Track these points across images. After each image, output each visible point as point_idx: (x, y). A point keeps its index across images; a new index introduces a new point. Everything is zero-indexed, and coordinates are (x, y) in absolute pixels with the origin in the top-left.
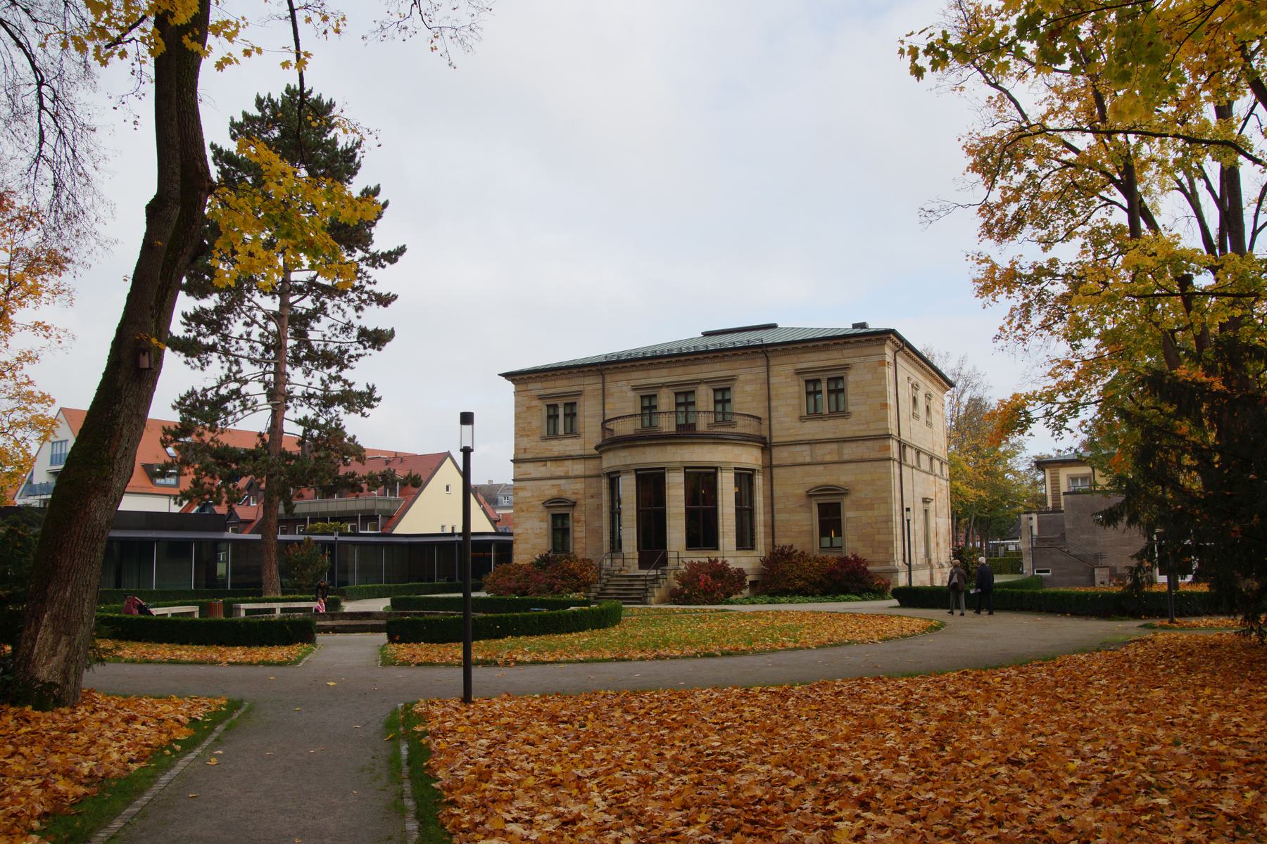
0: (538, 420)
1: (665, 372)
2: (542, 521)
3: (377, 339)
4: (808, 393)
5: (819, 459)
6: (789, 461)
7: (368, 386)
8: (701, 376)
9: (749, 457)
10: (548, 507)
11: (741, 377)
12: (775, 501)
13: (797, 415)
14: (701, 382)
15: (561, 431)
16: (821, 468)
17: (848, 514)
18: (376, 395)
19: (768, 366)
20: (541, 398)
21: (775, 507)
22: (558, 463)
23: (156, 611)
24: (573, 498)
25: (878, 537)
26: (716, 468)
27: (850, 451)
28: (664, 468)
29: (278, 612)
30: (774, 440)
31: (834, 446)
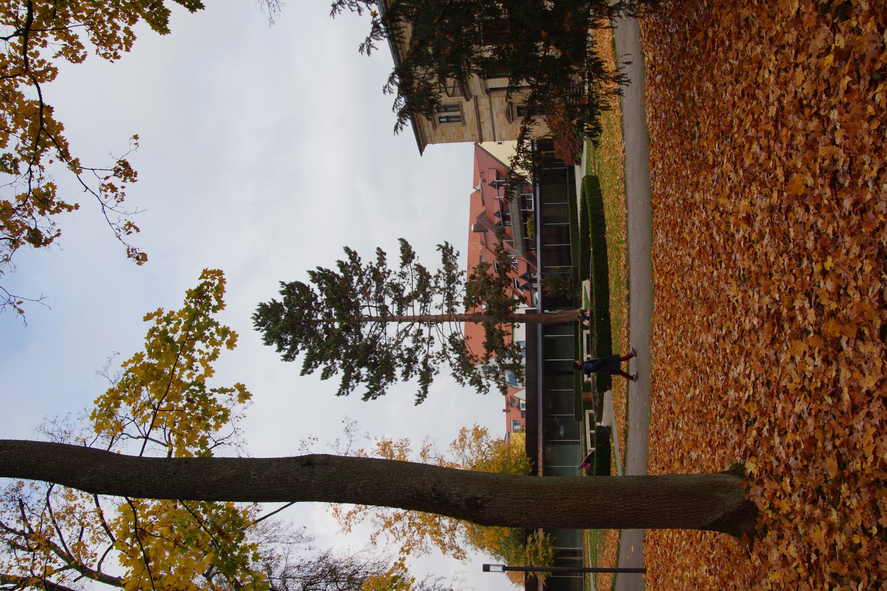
0: (452, 128)
3: (407, 254)
7: (438, 250)
10: (513, 119)
15: (458, 114)
18: (444, 244)
23: (586, 284)
29: (589, 356)
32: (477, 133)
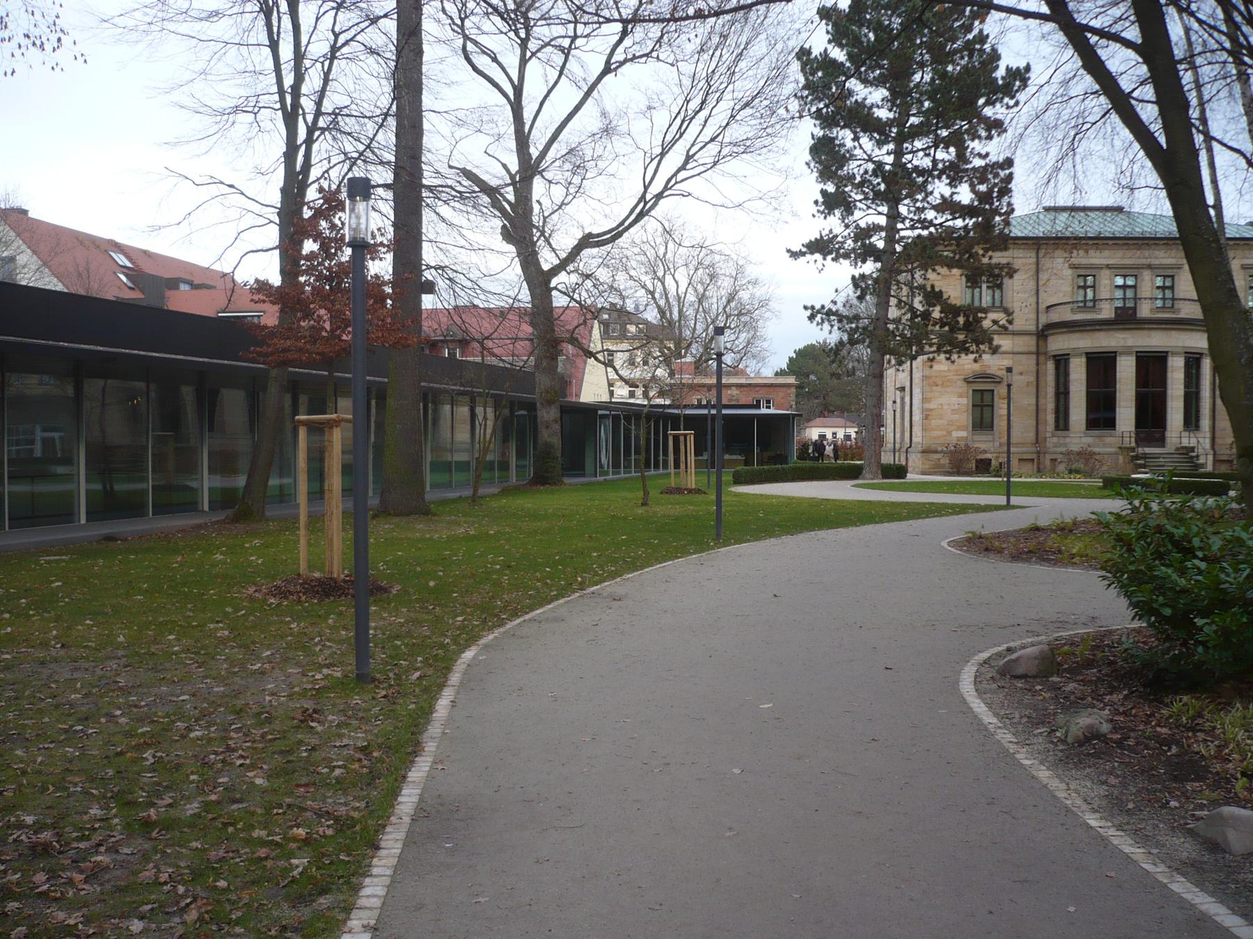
2: (961, 396)
28: (1167, 352)
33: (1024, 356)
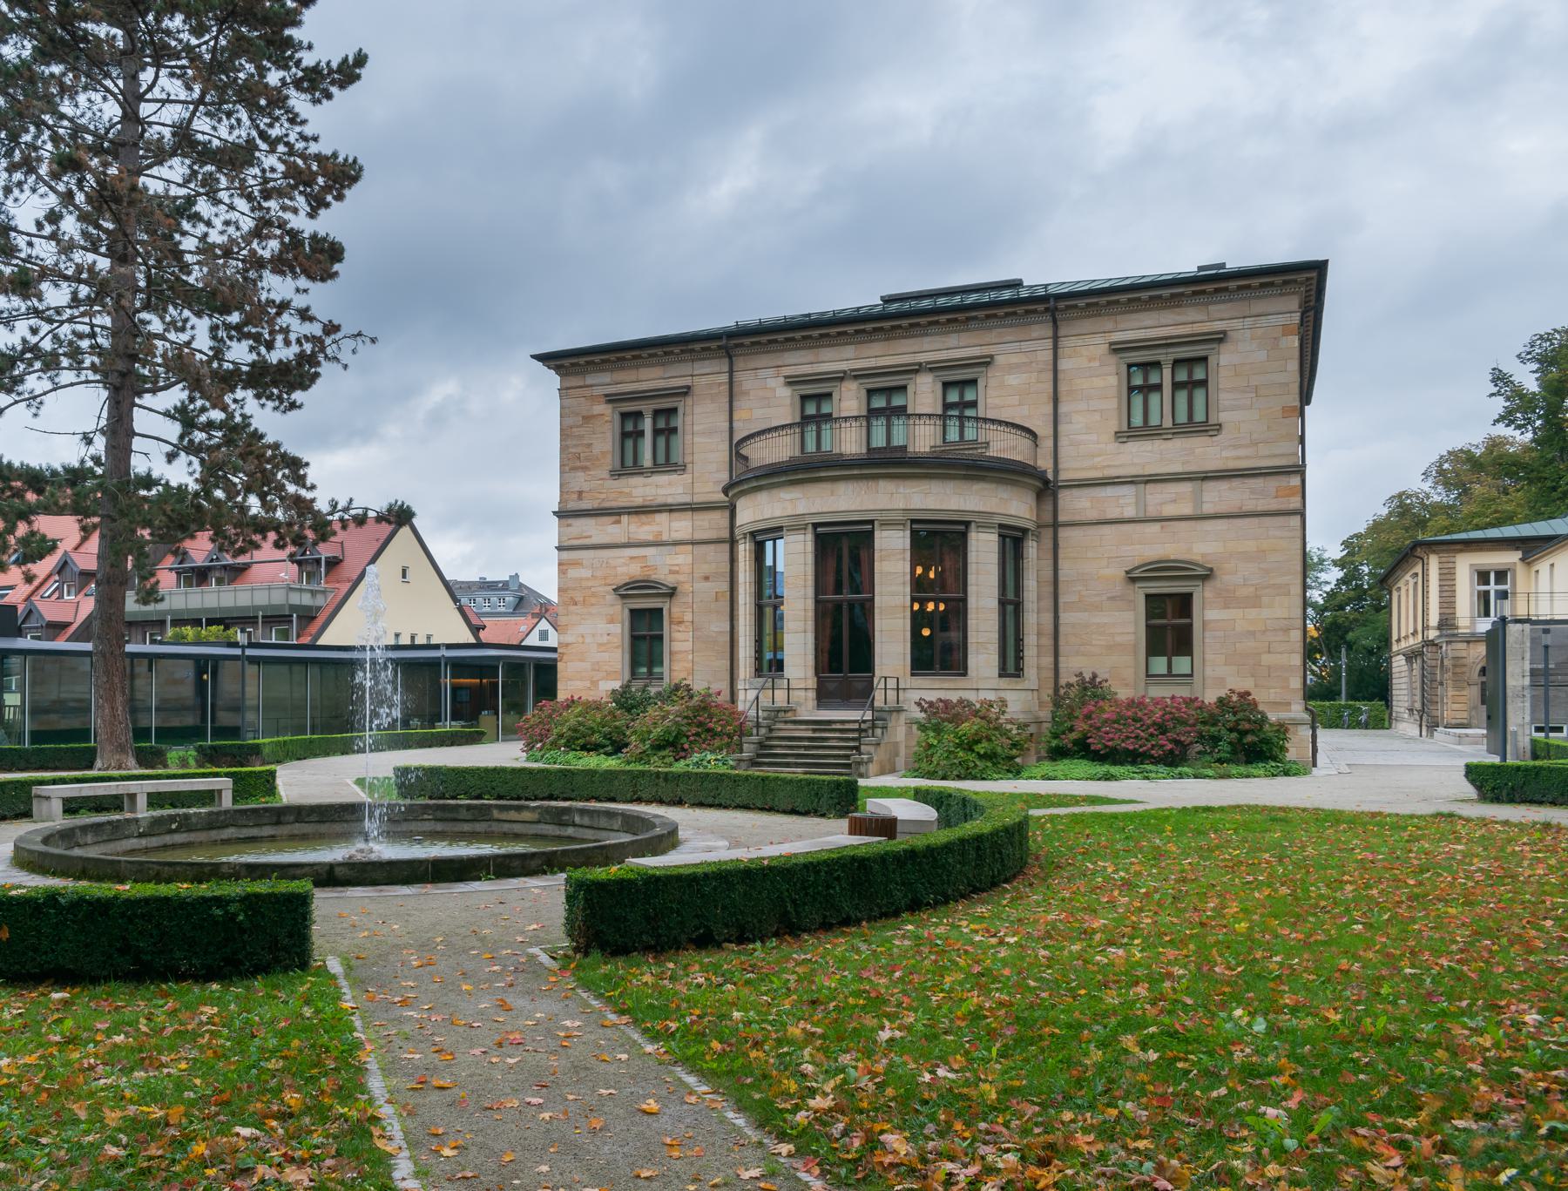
0: (604, 441)
1: (849, 351)
2: (611, 621)
4: (1131, 389)
5: (1152, 512)
6: (1093, 515)
8: (922, 358)
9: (1017, 506)
10: (623, 597)
11: (1000, 360)
12: (1061, 587)
13: (1114, 425)
14: (916, 369)
15: (647, 460)
16: (1156, 527)
17: (1209, 614)
19: (1056, 339)
20: (612, 399)
21: (1062, 600)
22: (643, 518)
24: (670, 580)
25: (1266, 659)
26: (967, 524)
27: (1218, 496)
28: (871, 522)
30: (1063, 476)
31: (1186, 487)
32: (586, 505)
33: (712, 547)
